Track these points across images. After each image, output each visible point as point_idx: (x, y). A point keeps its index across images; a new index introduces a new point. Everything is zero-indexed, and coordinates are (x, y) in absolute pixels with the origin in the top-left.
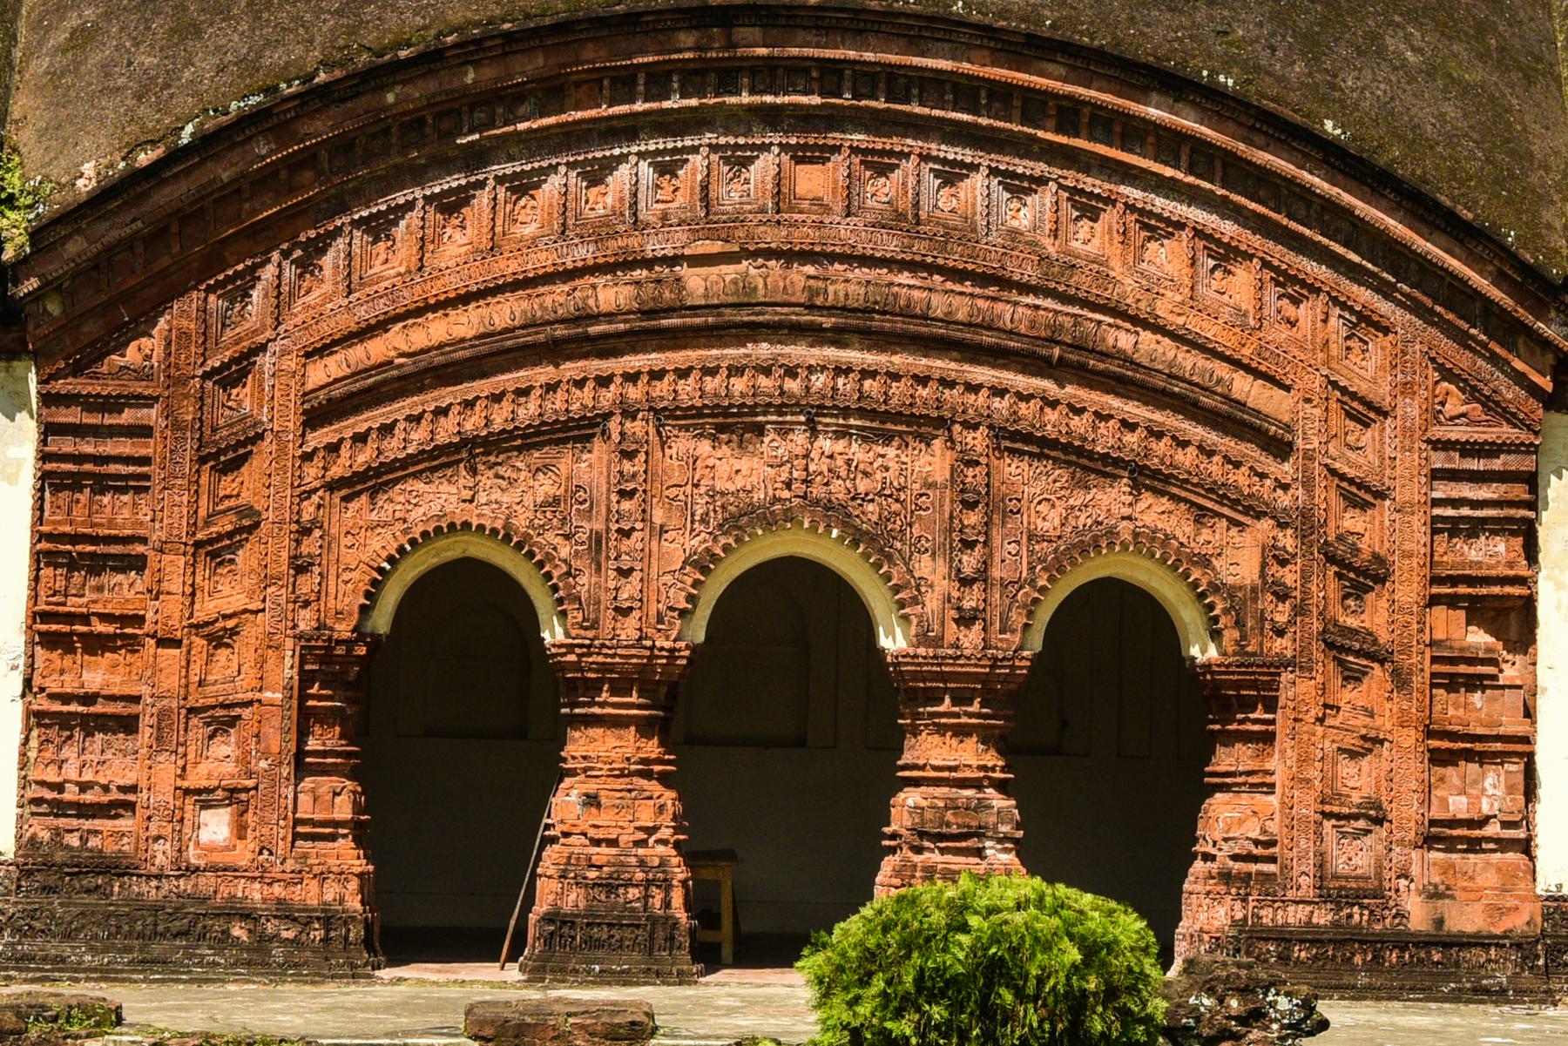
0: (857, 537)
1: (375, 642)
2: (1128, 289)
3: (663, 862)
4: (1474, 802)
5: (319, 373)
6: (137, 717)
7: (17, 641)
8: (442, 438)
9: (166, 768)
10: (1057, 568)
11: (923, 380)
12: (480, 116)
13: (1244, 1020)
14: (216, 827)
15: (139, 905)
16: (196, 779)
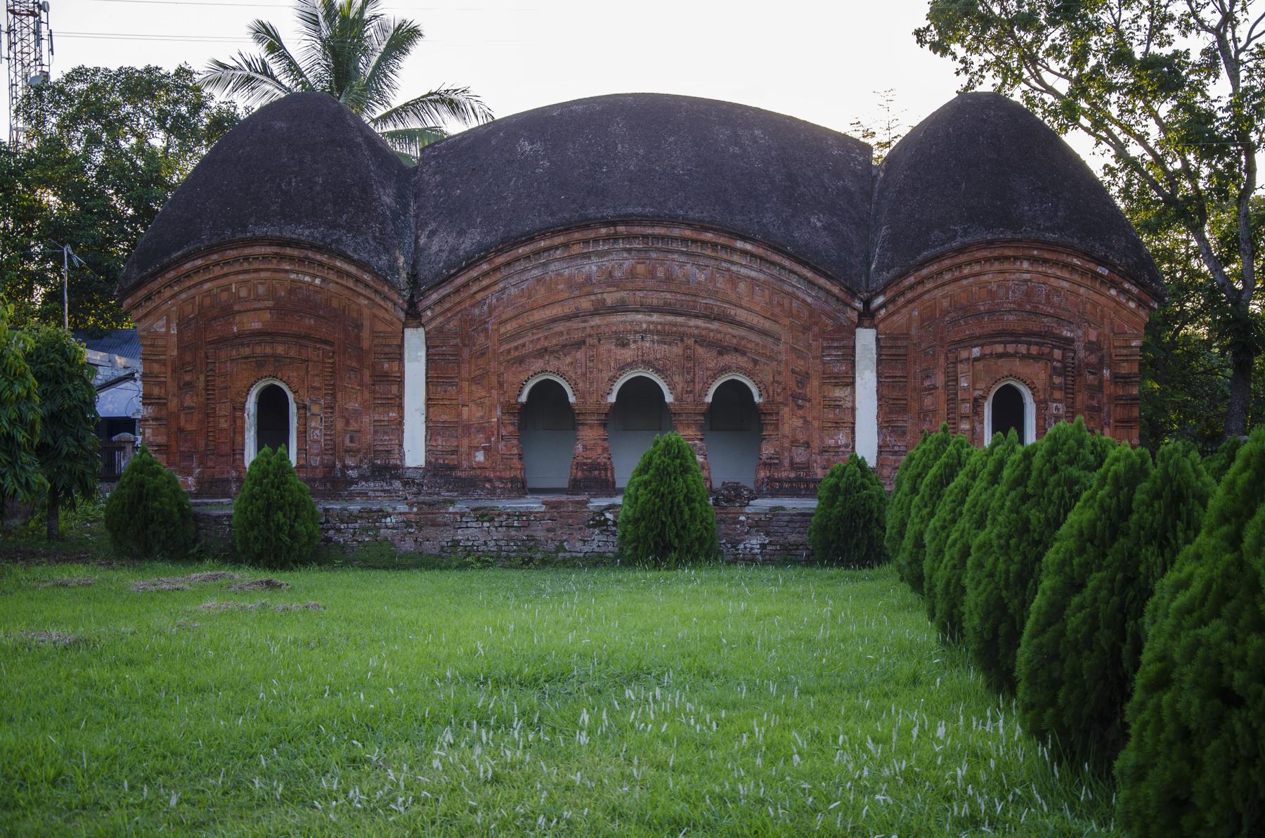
0: (657, 371)
1: (522, 404)
2: (733, 297)
3: (605, 464)
5: (502, 330)
7: (423, 407)
9: (465, 442)
10: (714, 377)
11: (675, 325)
12: (546, 254)
13: (735, 496)
14: (480, 457)
16: (475, 443)
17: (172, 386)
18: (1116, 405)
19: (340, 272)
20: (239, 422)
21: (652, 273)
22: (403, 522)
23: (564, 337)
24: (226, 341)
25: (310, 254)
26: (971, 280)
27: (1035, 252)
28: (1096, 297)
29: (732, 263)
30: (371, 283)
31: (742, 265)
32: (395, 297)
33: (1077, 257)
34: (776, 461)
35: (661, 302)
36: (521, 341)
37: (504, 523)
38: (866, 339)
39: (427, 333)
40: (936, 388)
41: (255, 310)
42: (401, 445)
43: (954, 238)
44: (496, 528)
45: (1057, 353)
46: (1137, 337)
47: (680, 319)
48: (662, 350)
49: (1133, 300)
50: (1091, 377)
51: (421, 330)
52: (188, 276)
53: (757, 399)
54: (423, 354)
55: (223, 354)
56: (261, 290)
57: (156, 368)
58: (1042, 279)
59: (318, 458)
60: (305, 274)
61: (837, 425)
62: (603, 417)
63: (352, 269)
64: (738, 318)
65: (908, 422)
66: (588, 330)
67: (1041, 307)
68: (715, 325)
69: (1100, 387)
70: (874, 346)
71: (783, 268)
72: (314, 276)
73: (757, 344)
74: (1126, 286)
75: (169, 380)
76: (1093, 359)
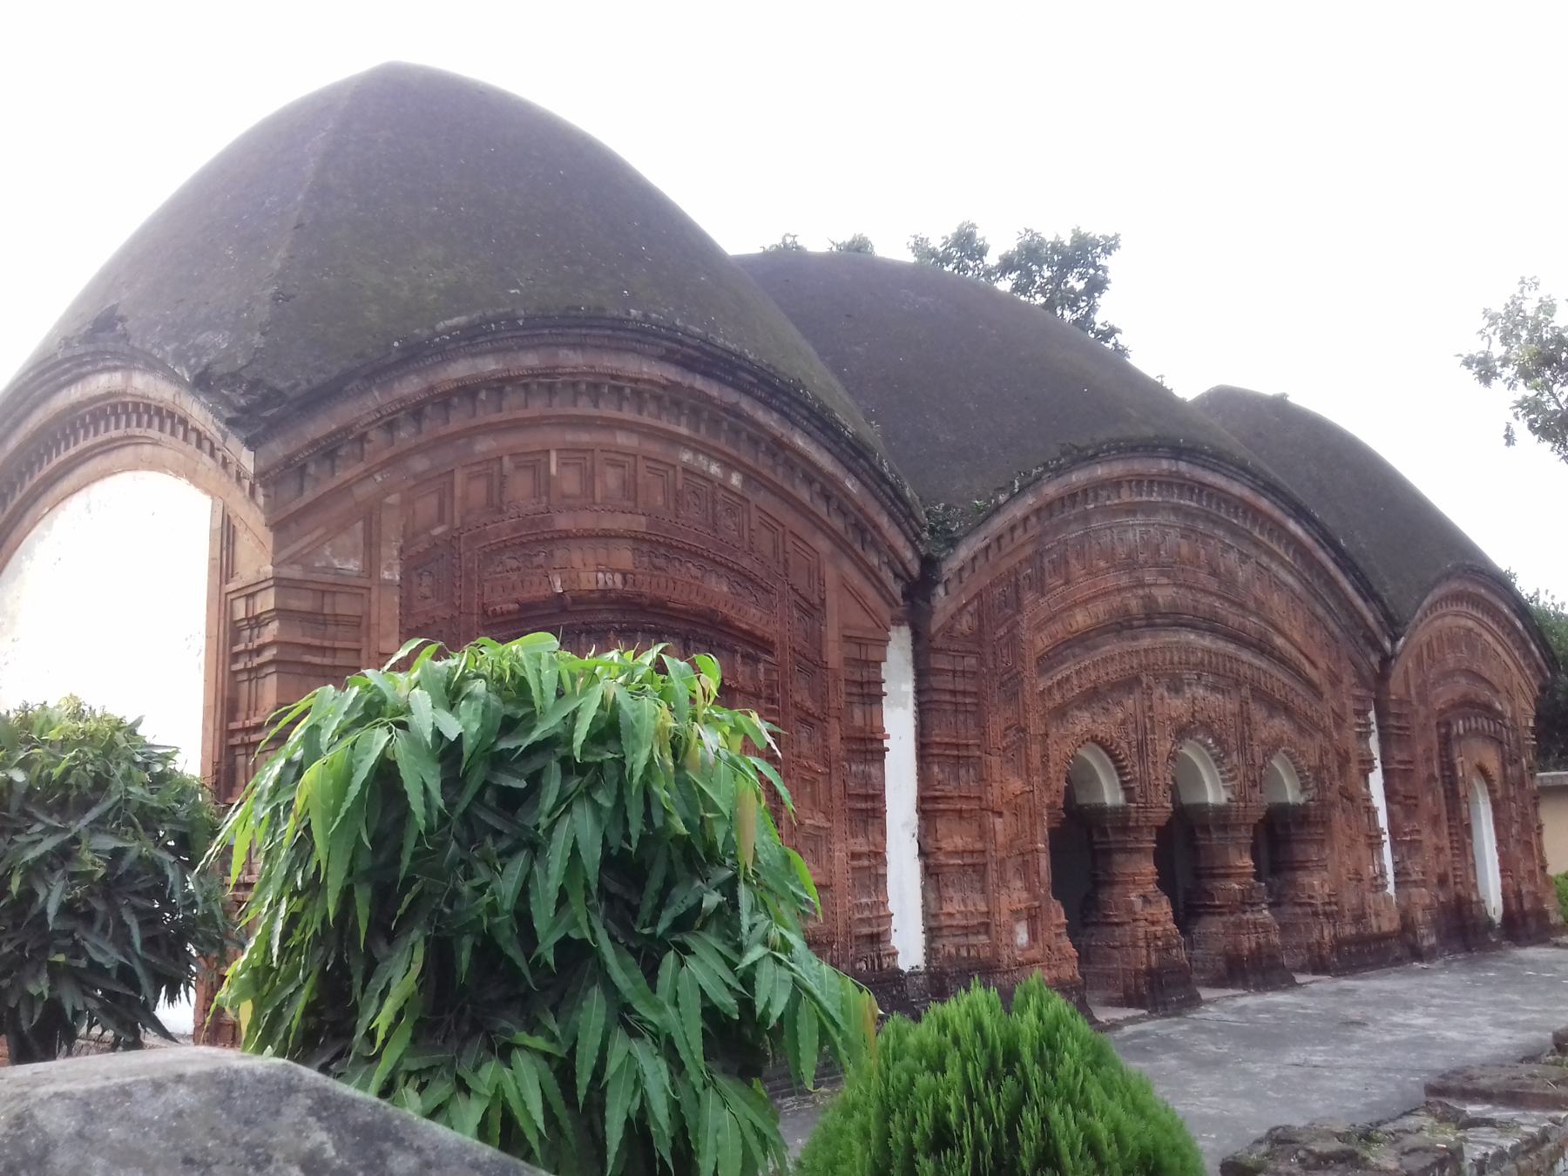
5: (1042, 642)
6: (985, 865)
7: (915, 818)
14: (1022, 937)
25: (746, 405)
27: (1483, 591)
29: (1272, 554)
31: (1283, 563)
32: (900, 542)
34: (1335, 908)
47: (1231, 648)
52: (443, 400)
54: (908, 687)
58: (1477, 629)
60: (712, 453)
63: (824, 460)
68: (1263, 664)
71: (1322, 570)
72: (730, 464)
74: (1533, 647)
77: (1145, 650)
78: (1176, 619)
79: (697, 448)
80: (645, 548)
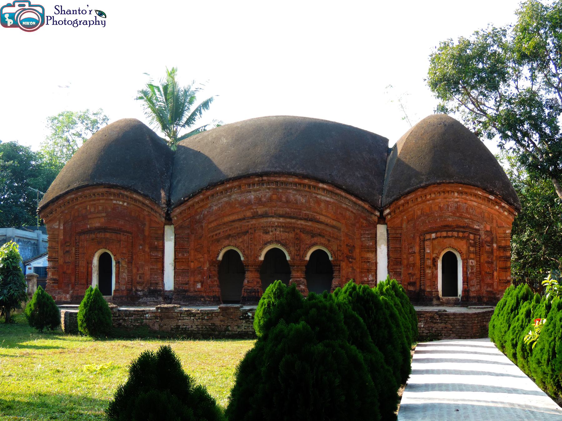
1: (219, 261)
3: (258, 289)
4: (368, 279)
5: (210, 226)
7: (173, 262)
8: (226, 234)
9: (192, 279)
10: (309, 248)
11: (291, 223)
12: (230, 190)
14: (199, 286)
15: (189, 297)
16: (197, 279)
17: (61, 253)
18: (500, 261)
19: (136, 200)
20: (90, 269)
21: (280, 199)
22: (154, 316)
23: (239, 229)
24: (84, 232)
25: (122, 192)
26: (431, 202)
27: (460, 189)
28: (489, 209)
29: (318, 194)
30: (149, 205)
31: (322, 195)
32: (160, 211)
33: (480, 191)
35: (284, 213)
36: (218, 232)
37: (200, 317)
38: (381, 230)
39: (175, 228)
40: (415, 253)
41: (97, 217)
42: (163, 281)
43: (421, 182)
44: (197, 320)
45: (472, 236)
46: (509, 228)
47: (293, 221)
48: (285, 235)
49: (506, 211)
50: (488, 247)
51: (172, 226)
53: (330, 258)
55: (83, 237)
56: (100, 208)
57: (54, 244)
58: (464, 201)
59: (125, 286)
60: (120, 201)
61: (369, 271)
62: (257, 267)
63: (141, 198)
64: (321, 220)
65: (402, 270)
66: (250, 226)
67: (464, 214)
68: (310, 224)
69: (492, 252)
70: (385, 233)
71: (342, 196)
72: (124, 202)
73: (330, 233)
74: (503, 204)
75: (59, 250)
76: (488, 239)
77: (252, 225)
78: (265, 215)
79: (117, 201)
80: (105, 218)
